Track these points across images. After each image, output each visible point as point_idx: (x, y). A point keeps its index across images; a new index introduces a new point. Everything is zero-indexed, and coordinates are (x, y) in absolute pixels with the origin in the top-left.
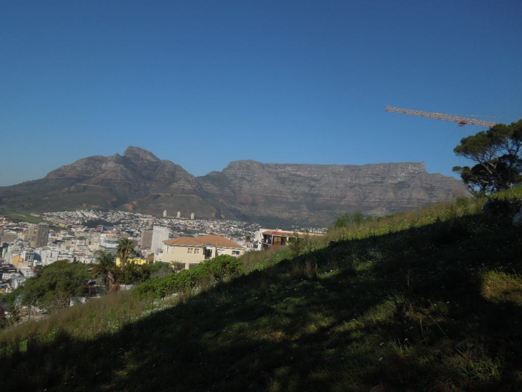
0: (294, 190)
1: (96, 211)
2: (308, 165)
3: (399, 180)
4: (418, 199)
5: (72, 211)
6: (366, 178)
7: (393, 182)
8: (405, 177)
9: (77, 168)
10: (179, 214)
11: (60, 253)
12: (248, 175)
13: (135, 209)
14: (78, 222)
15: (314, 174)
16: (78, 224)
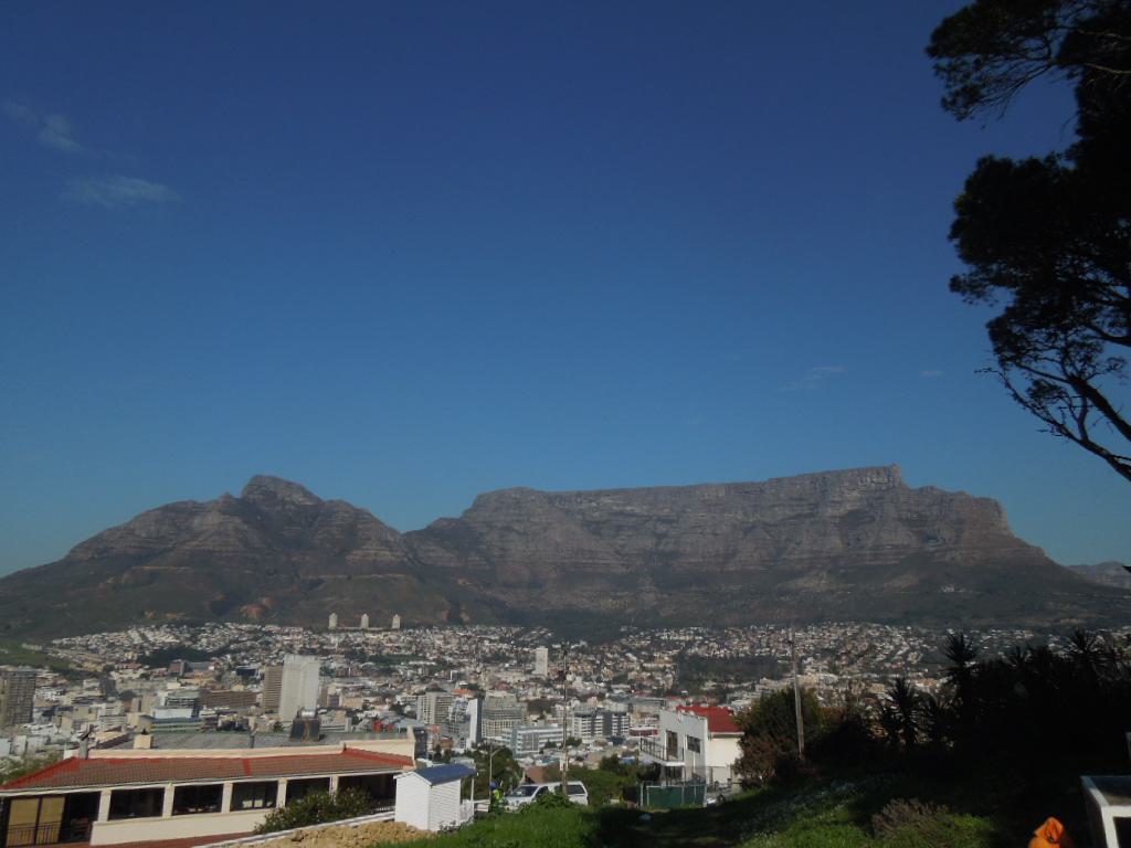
0: (623, 546)
1: (175, 625)
2: (649, 489)
3: (849, 507)
4: (895, 547)
5: (118, 630)
6: (777, 509)
7: (836, 512)
8: (861, 499)
9: (137, 532)
10: (365, 619)
11: (49, 740)
12: (518, 521)
13: (265, 617)
14: (129, 656)
15: (663, 509)
16: (128, 661)
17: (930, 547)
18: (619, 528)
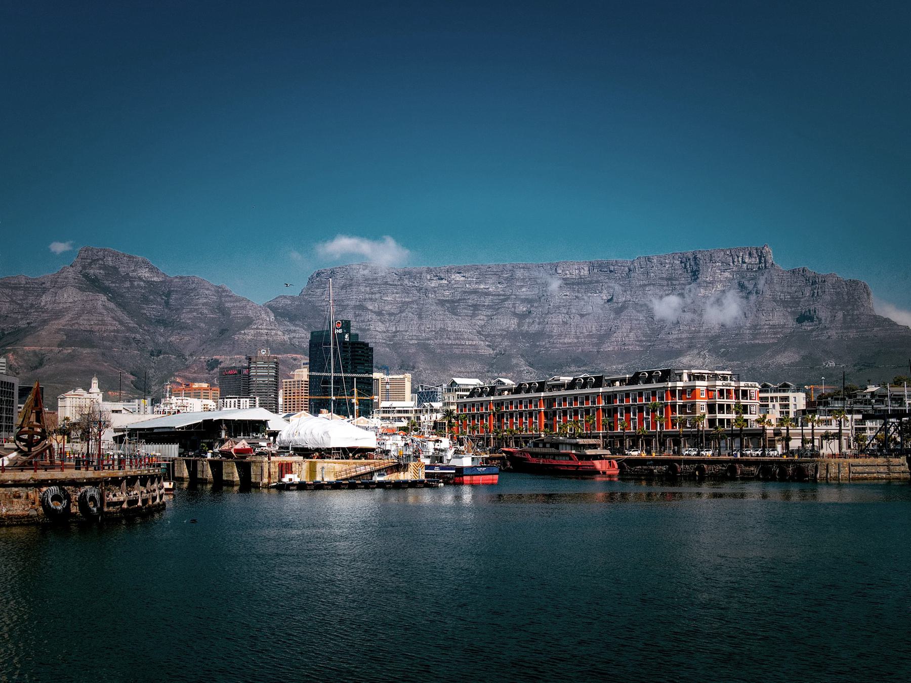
4: (773, 327)
12: (371, 299)
17: (807, 326)
18: (476, 307)
